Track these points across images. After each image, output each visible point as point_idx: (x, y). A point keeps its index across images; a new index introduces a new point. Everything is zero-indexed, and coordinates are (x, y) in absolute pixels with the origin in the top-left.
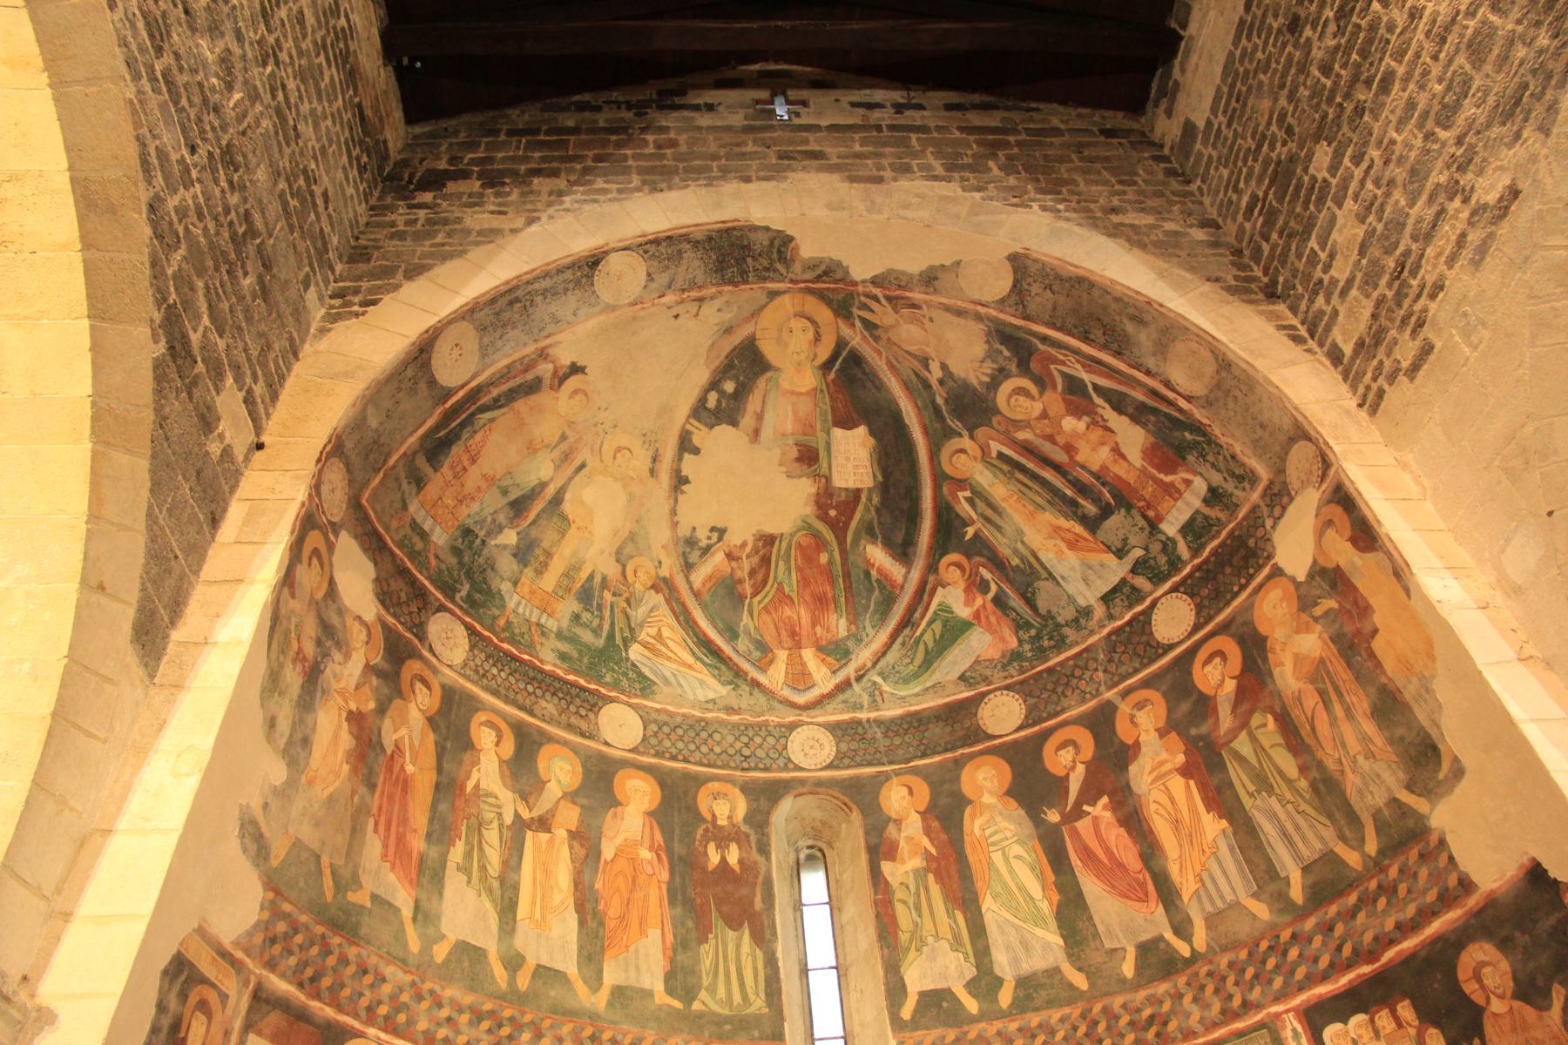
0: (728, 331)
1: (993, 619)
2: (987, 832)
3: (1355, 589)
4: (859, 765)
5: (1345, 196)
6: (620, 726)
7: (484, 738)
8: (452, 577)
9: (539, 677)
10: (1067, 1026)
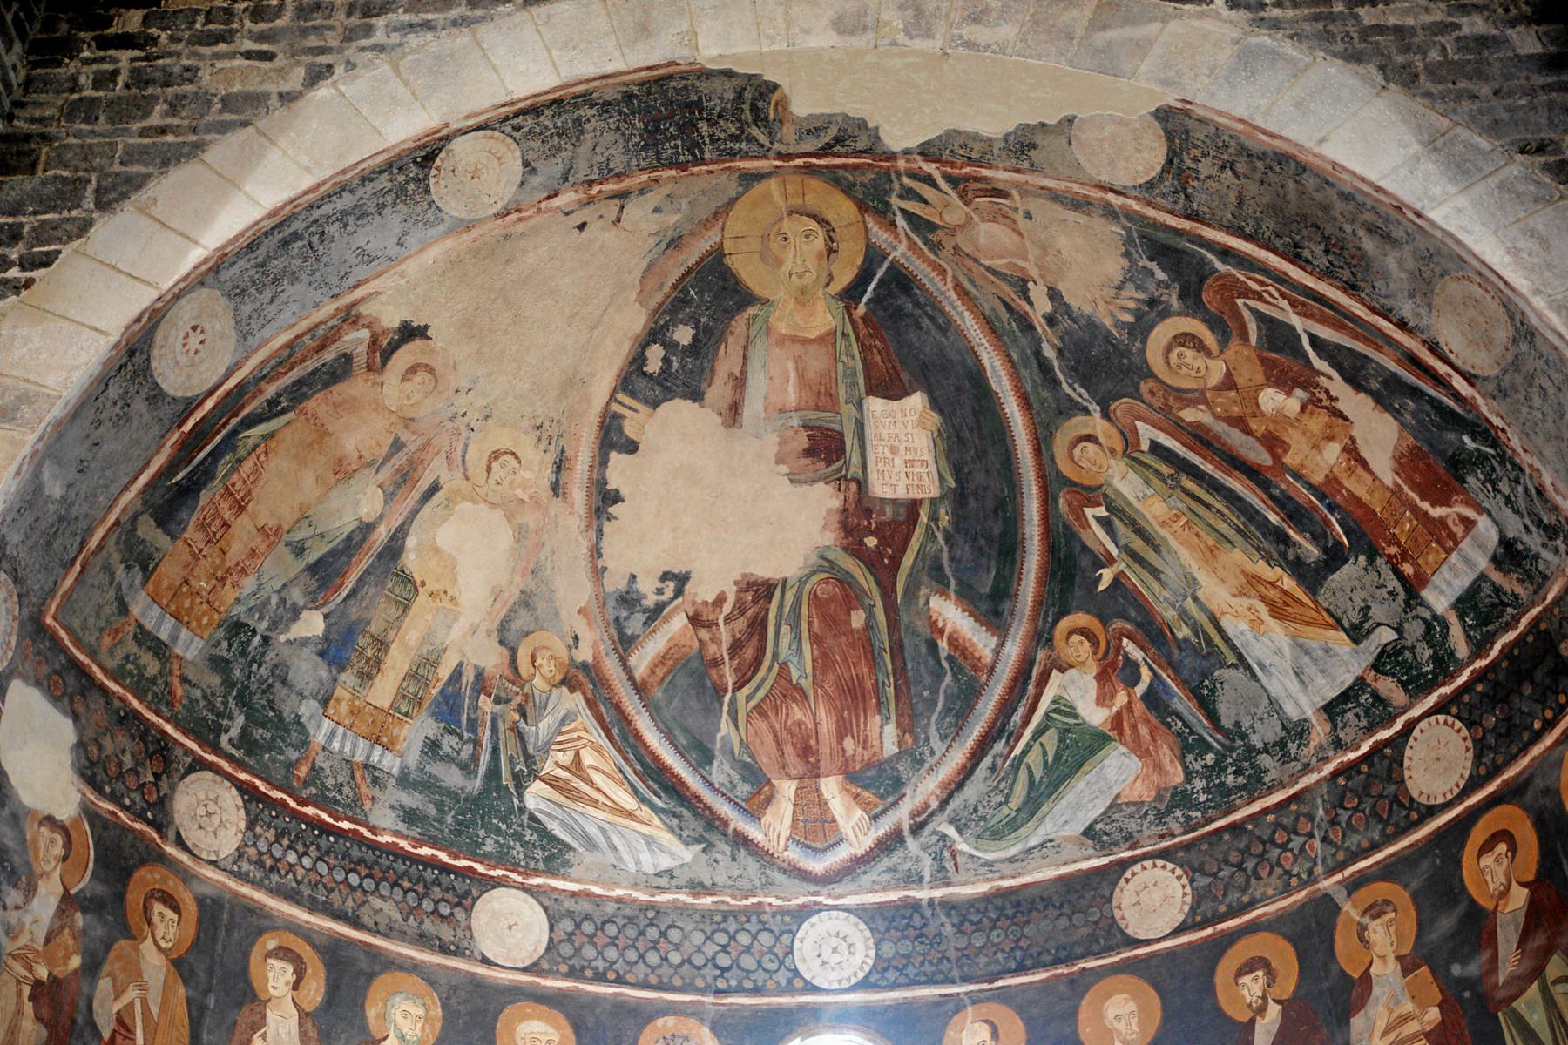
0: (675, 243)
1: (1144, 731)
4: (913, 983)
6: (510, 927)
7: (276, 978)
8: (211, 707)
9: (370, 856)
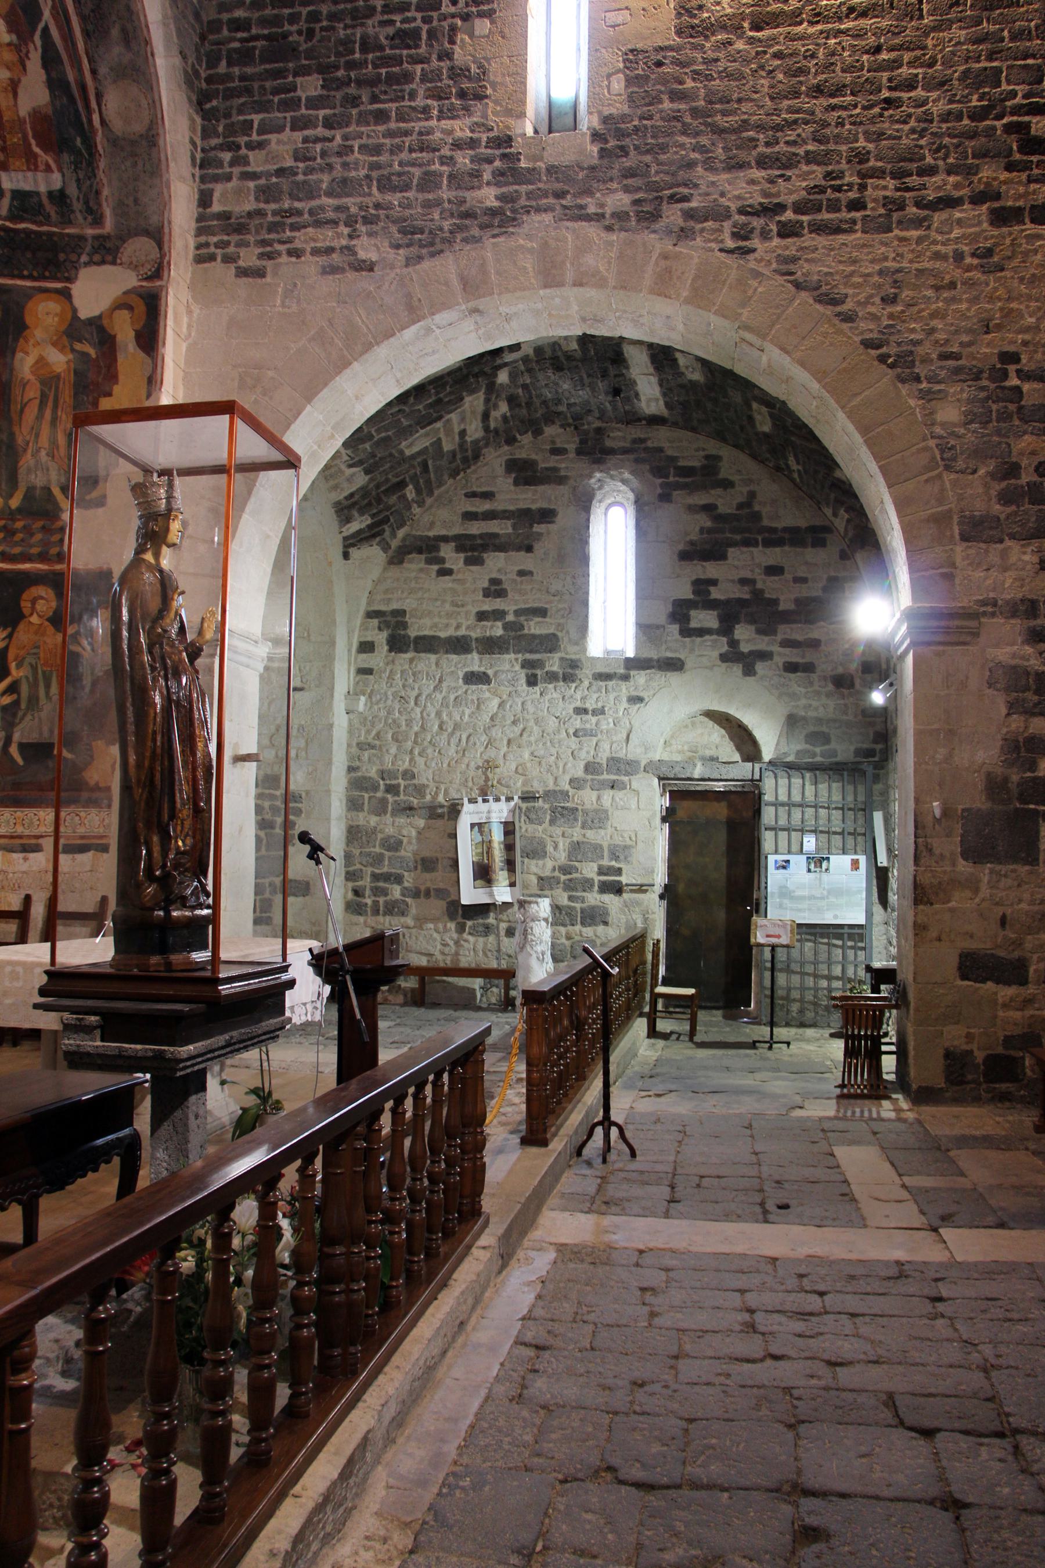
3: (116, 360)
5: (302, 129)
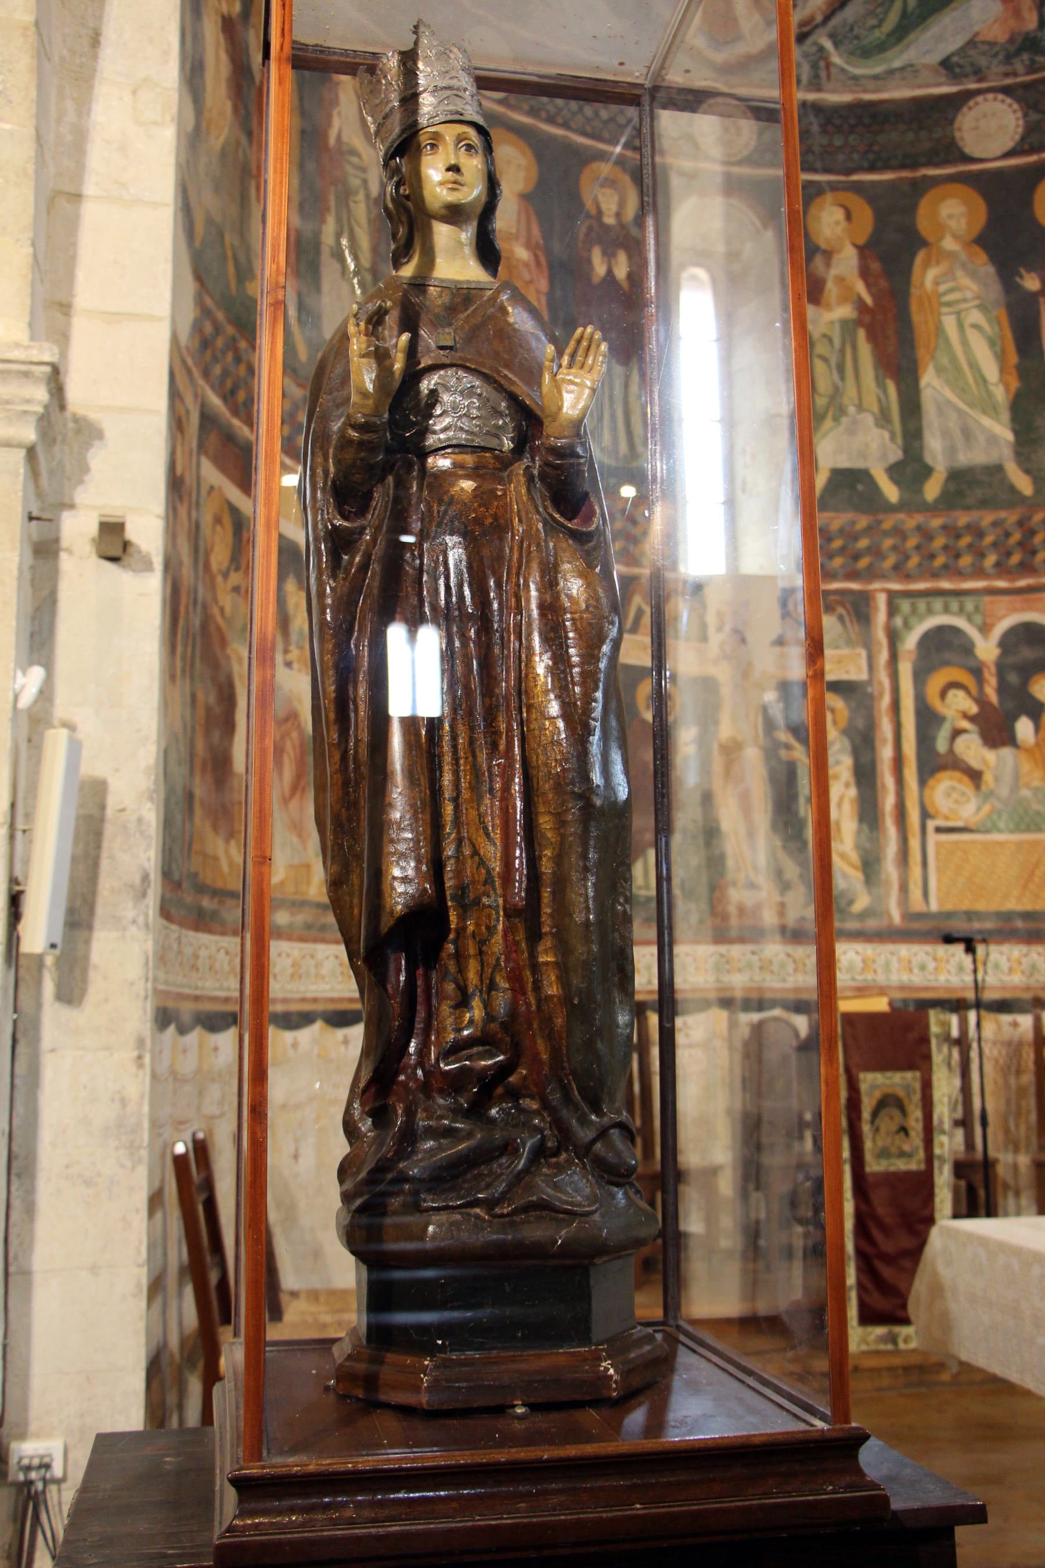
2: (942, 288)
10: (999, 531)
